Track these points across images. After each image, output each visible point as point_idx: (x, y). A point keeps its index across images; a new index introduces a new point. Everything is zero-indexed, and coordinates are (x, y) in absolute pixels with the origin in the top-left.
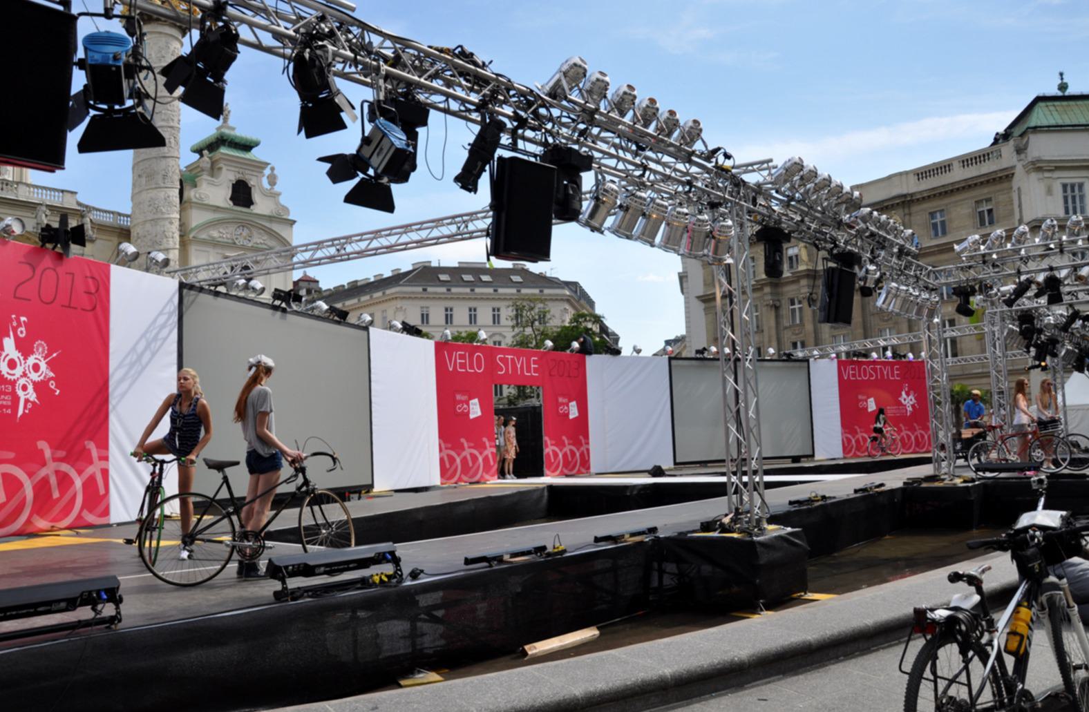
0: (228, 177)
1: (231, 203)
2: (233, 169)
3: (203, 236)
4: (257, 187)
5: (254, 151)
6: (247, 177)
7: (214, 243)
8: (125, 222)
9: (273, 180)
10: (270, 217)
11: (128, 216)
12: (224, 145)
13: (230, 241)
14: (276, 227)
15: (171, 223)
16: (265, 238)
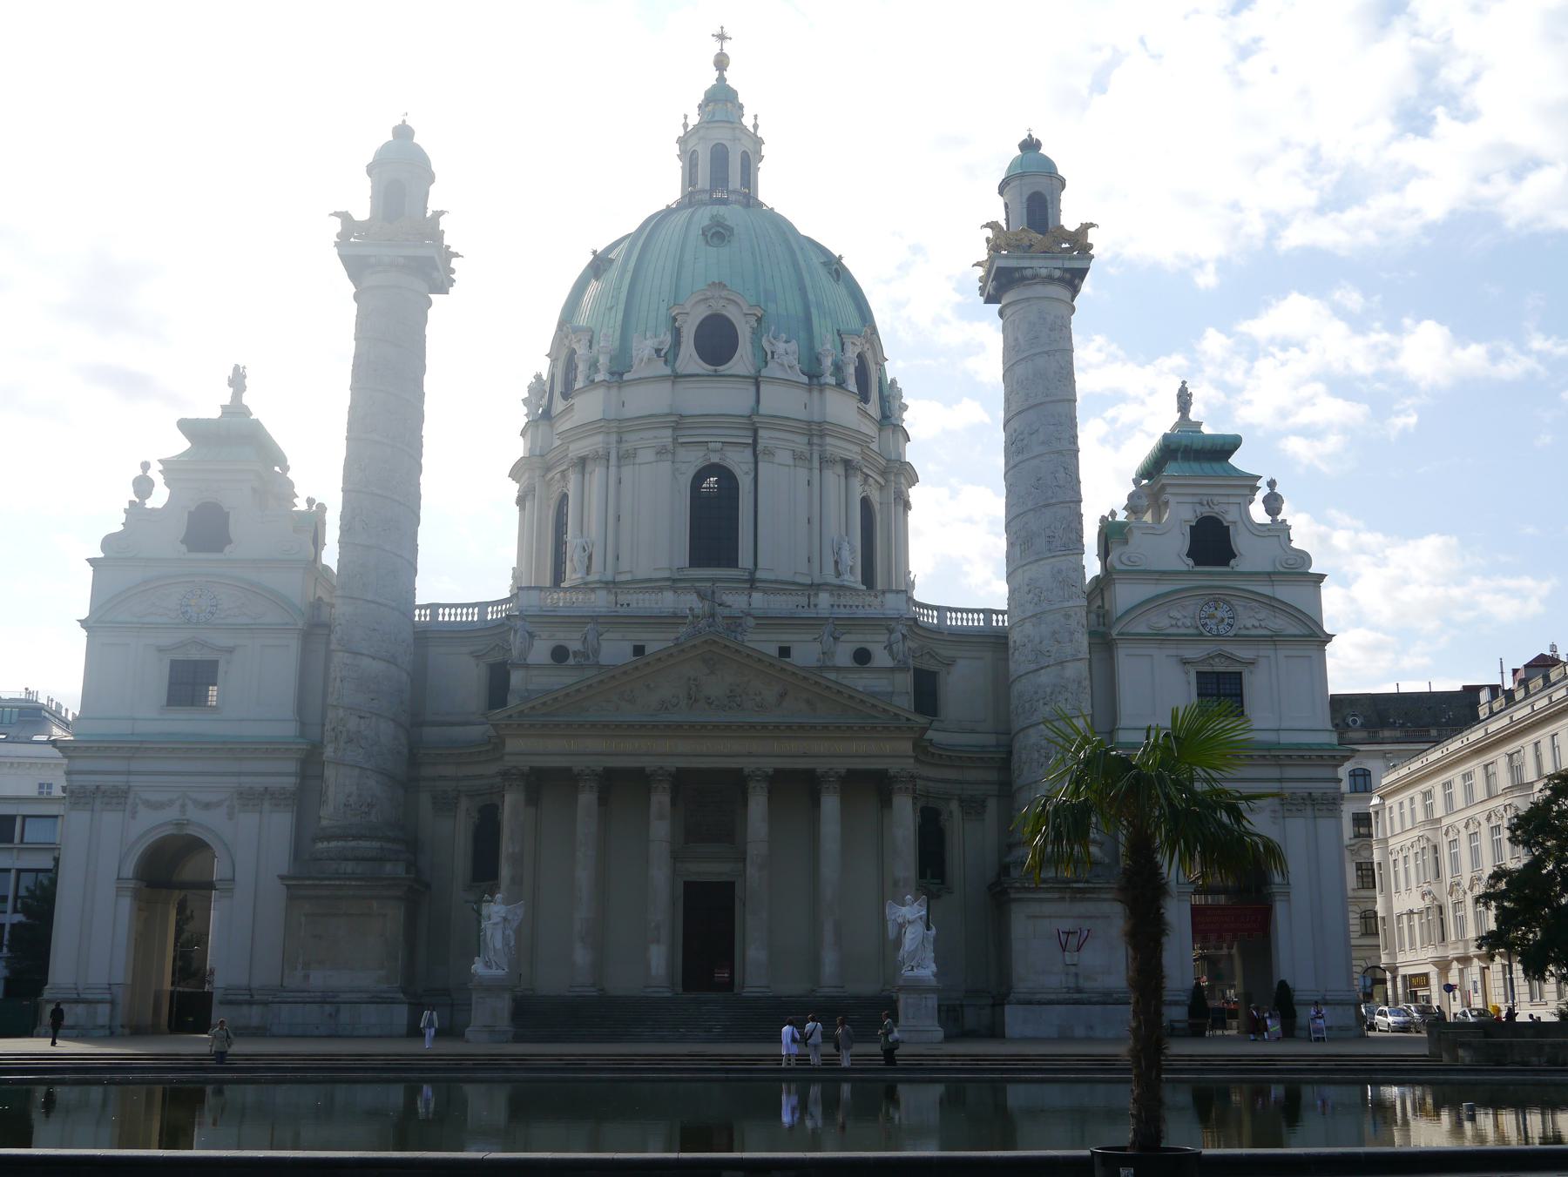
0: (1180, 515)
1: (1190, 562)
2: (1189, 499)
3: (1142, 629)
4: (1240, 524)
5: (1234, 460)
6: (1216, 509)
7: (1160, 638)
8: (1000, 621)
9: (1273, 504)
10: (1269, 574)
11: (1003, 613)
12: (1175, 459)
13: (1192, 631)
14: (1285, 593)
15: (1067, 616)
16: (1263, 613)
